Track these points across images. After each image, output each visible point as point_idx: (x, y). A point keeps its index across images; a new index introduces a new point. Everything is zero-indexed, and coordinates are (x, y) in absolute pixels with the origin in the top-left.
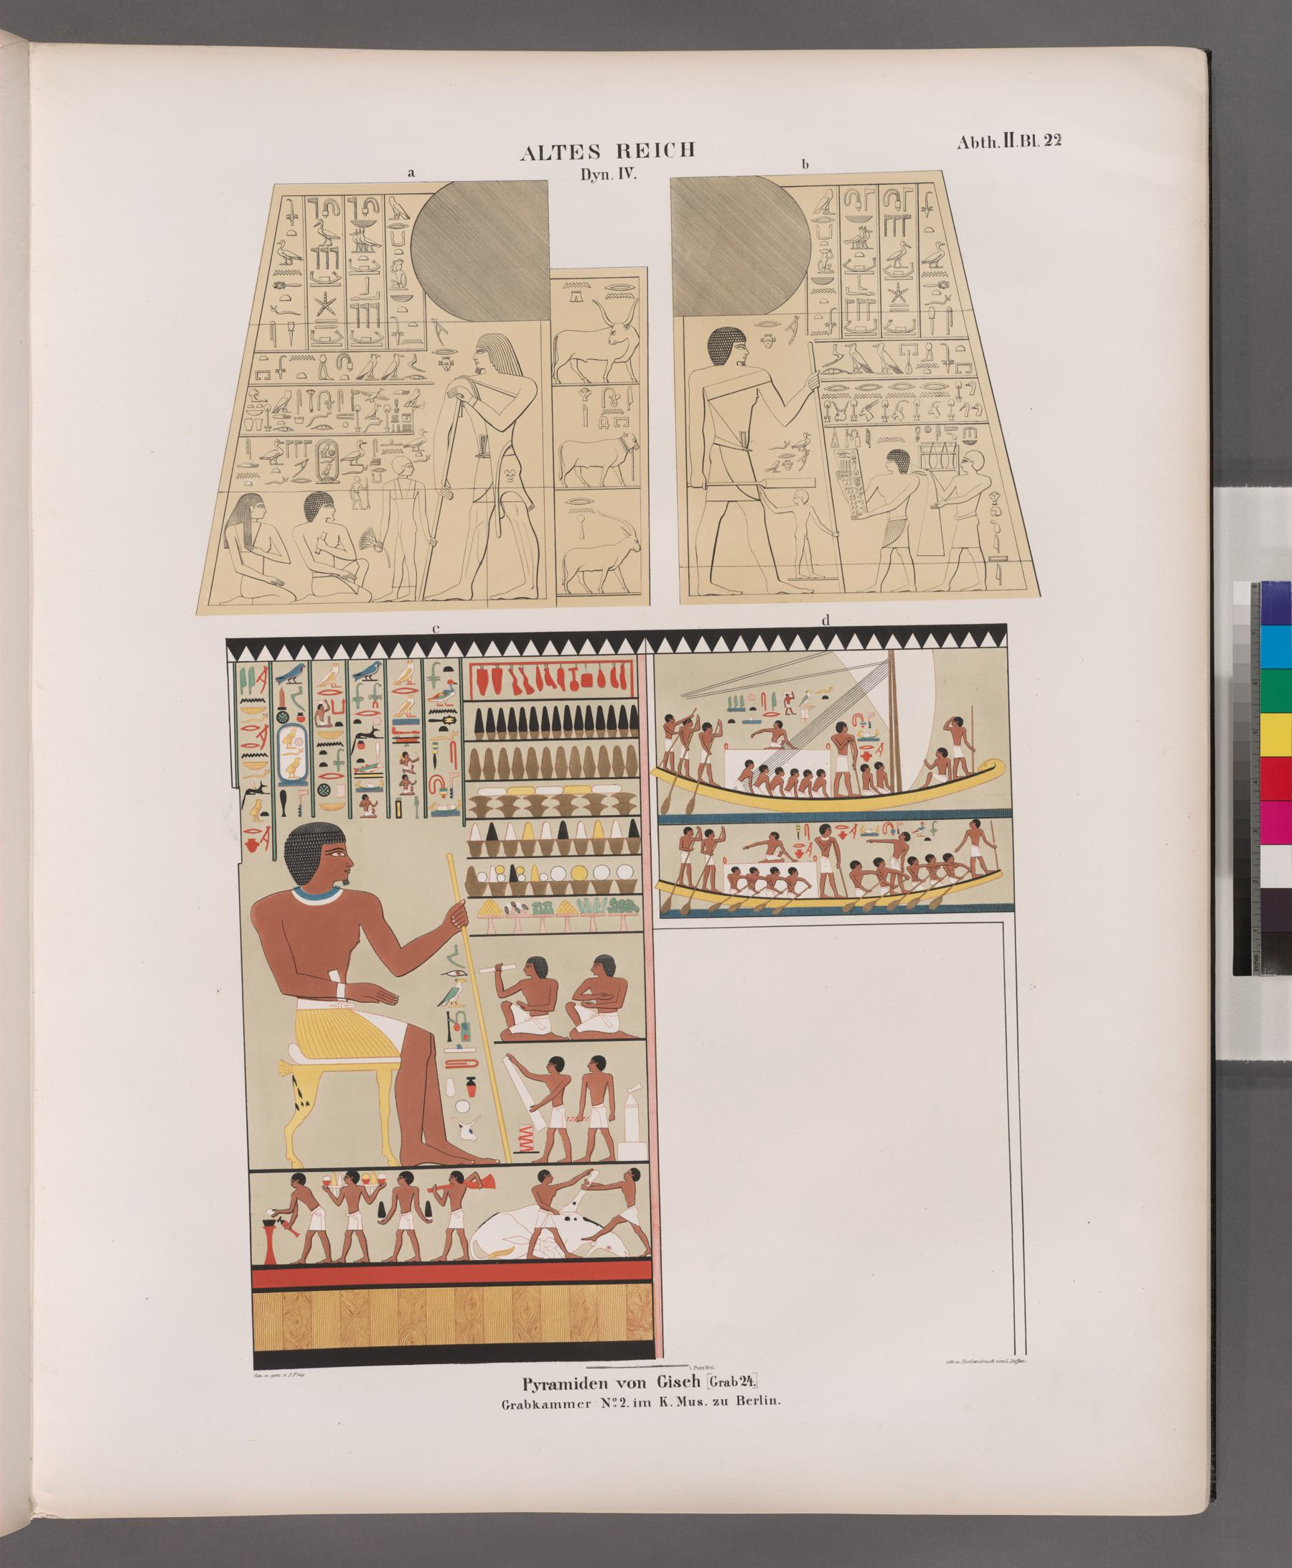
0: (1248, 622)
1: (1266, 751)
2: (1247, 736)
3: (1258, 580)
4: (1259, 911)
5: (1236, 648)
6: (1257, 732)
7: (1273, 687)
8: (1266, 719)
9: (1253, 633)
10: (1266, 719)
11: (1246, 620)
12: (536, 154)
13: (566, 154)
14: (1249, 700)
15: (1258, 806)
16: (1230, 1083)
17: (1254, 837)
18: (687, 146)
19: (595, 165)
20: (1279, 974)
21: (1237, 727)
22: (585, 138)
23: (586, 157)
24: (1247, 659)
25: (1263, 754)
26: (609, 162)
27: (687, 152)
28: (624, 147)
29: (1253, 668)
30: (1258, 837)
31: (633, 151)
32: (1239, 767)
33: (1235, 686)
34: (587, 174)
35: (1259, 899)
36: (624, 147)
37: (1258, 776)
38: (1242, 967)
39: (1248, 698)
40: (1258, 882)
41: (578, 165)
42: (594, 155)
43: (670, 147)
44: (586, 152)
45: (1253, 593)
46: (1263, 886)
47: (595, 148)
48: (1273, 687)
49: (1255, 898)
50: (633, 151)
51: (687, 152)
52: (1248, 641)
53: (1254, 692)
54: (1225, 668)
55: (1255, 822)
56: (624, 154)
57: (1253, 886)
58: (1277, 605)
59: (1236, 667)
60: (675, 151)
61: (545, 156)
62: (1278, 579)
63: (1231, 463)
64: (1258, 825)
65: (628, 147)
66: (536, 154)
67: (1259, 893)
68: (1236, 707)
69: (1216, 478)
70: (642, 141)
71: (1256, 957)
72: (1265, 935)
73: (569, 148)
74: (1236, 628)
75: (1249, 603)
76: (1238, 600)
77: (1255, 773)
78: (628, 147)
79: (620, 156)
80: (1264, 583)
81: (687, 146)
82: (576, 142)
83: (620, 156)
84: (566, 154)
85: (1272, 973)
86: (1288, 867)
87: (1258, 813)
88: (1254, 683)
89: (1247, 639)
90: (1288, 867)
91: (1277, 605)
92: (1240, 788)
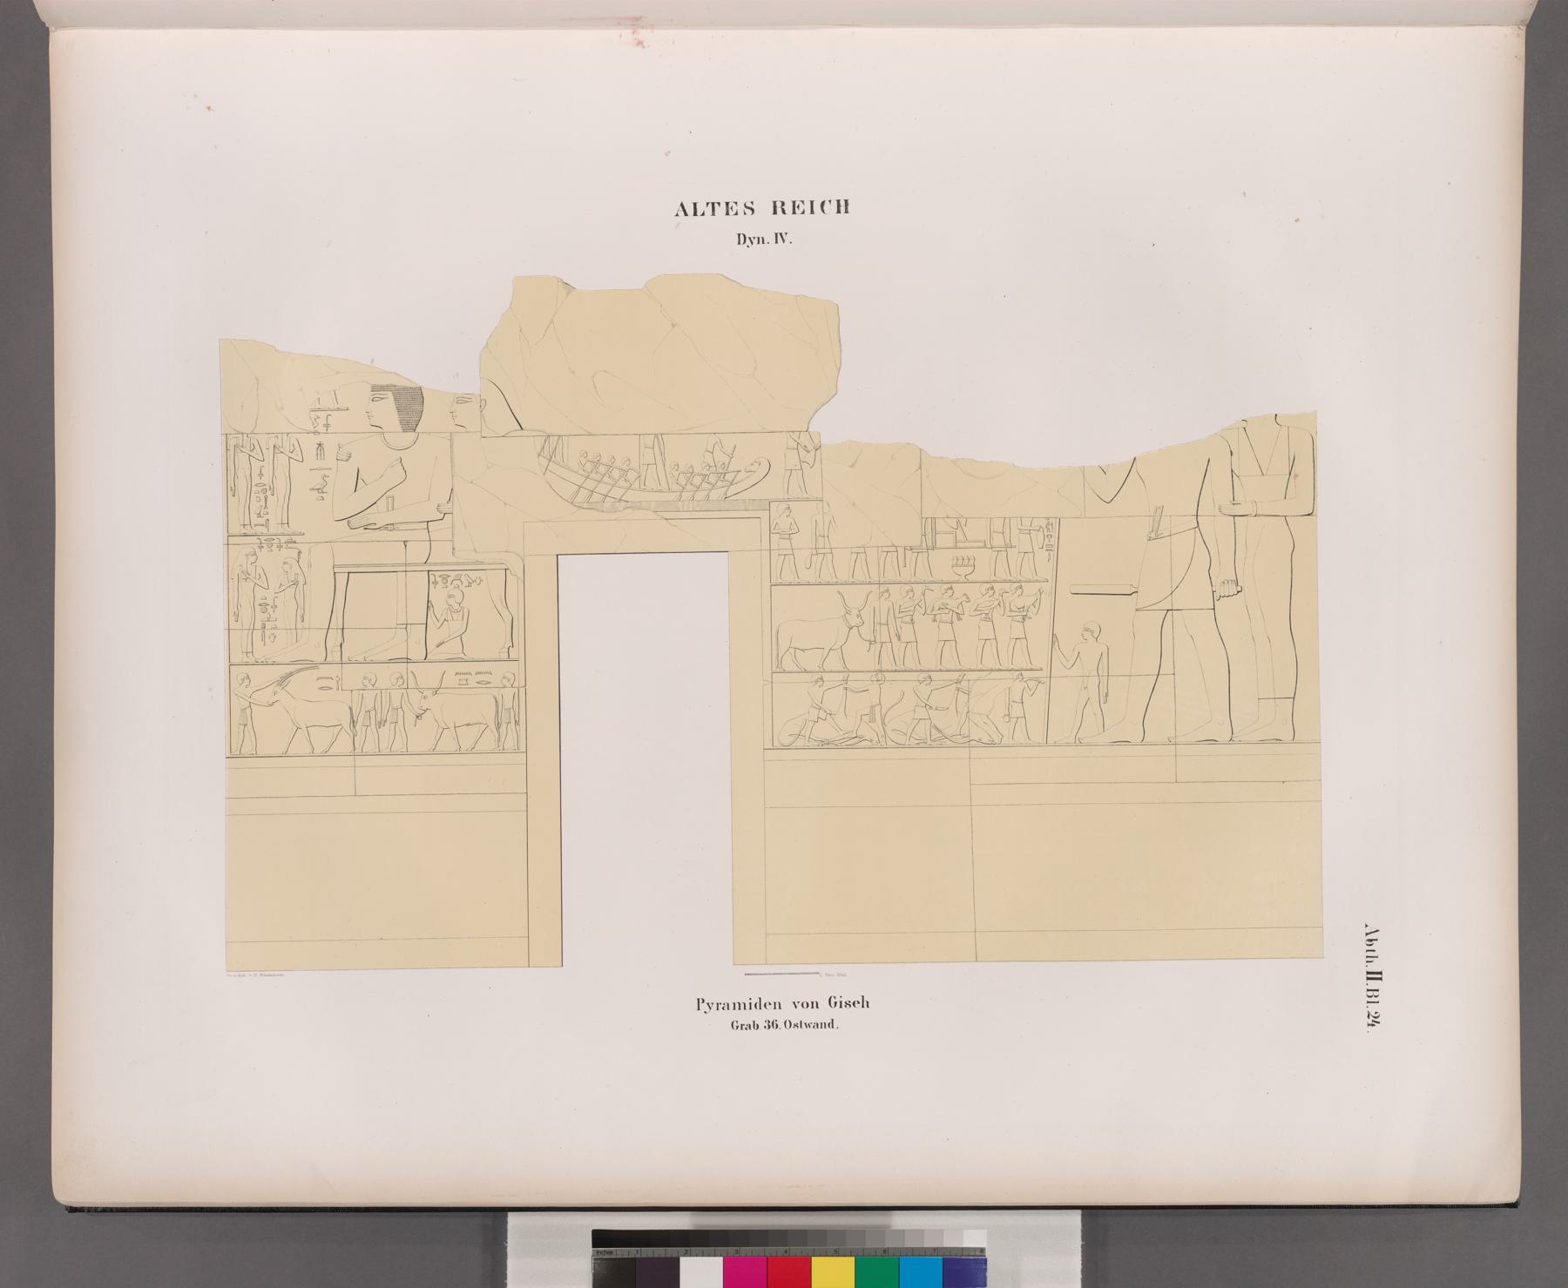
0: (946, 1245)
1: (816, 1262)
2: (832, 1243)
5: (920, 1233)
6: (836, 1253)
8: (850, 1262)
9: (935, 1251)
10: (850, 1262)
11: (949, 1242)
14: (868, 1246)
16: (488, 1222)
17: (731, 1251)
20: (594, 1275)
21: (841, 1234)
29: (900, 1249)
32: (801, 1236)
33: (882, 1231)
39: (870, 1244)
45: (975, 1249)
48: (883, 1271)
49: (670, 1252)
53: (876, 1250)
54: (899, 1221)
55: (746, 1251)
57: (682, 1249)
59: (901, 1233)
62: (989, 1274)
63: (1103, 1223)
68: (861, 1233)
69: (1087, 1210)
72: (633, 1261)
74: (940, 1233)
76: (968, 1234)
77: (796, 1251)
92: (782, 1236)
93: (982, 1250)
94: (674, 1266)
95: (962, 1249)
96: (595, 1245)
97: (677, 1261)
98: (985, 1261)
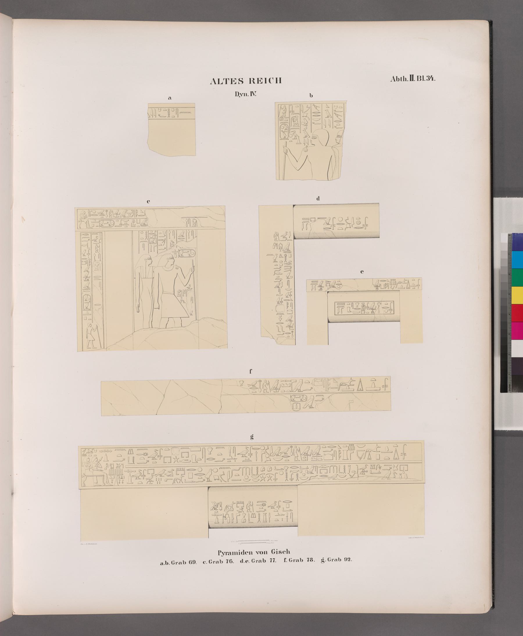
0: (507, 250)
1: (513, 302)
2: (506, 296)
4: (511, 367)
5: (502, 260)
6: (510, 294)
7: (517, 276)
8: (513, 288)
9: (509, 254)
10: (513, 288)
12: (217, 82)
13: (229, 82)
15: (510, 324)
17: (509, 337)
18: (278, 79)
20: (519, 392)
21: (502, 292)
22: (236, 76)
23: (237, 83)
24: (506, 265)
27: (278, 81)
28: (252, 80)
30: (510, 337)
31: (256, 81)
32: (503, 308)
33: (501, 276)
35: (511, 362)
36: (252, 80)
37: (510, 312)
38: (504, 389)
39: (506, 280)
40: (510, 355)
42: (241, 82)
43: (271, 80)
44: (237, 81)
46: (512, 357)
47: (241, 79)
48: (517, 276)
49: (509, 361)
50: (256, 81)
51: (278, 81)
52: (507, 257)
53: (509, 278)
55: (509, 330)
56: (252, 82)
57: (508, 356)
60: (273, 81)
61: (220, 83)
62: (519, 233)
64: (510, 332)
65: (254, 79)
67: (511, 359)
68: (502, 284)
71: (510, 385)
73: (230, 80)
74: (502, 252)
76: (502, 241)
77: (509, 311)
78: (254, 79)
79: (250, 83)
81: (278, 79)
83: (250, 83)
84: (229, 82)
85: (516, 392)
86: (522, 349)
87: (510, 327)
88: (509, 274)
89: (506, 257)
90: (522, 349)
92: (503, 316)
93: (509, 235)
96: (507, 392)
97: (513, 358)
98: (514, 234)
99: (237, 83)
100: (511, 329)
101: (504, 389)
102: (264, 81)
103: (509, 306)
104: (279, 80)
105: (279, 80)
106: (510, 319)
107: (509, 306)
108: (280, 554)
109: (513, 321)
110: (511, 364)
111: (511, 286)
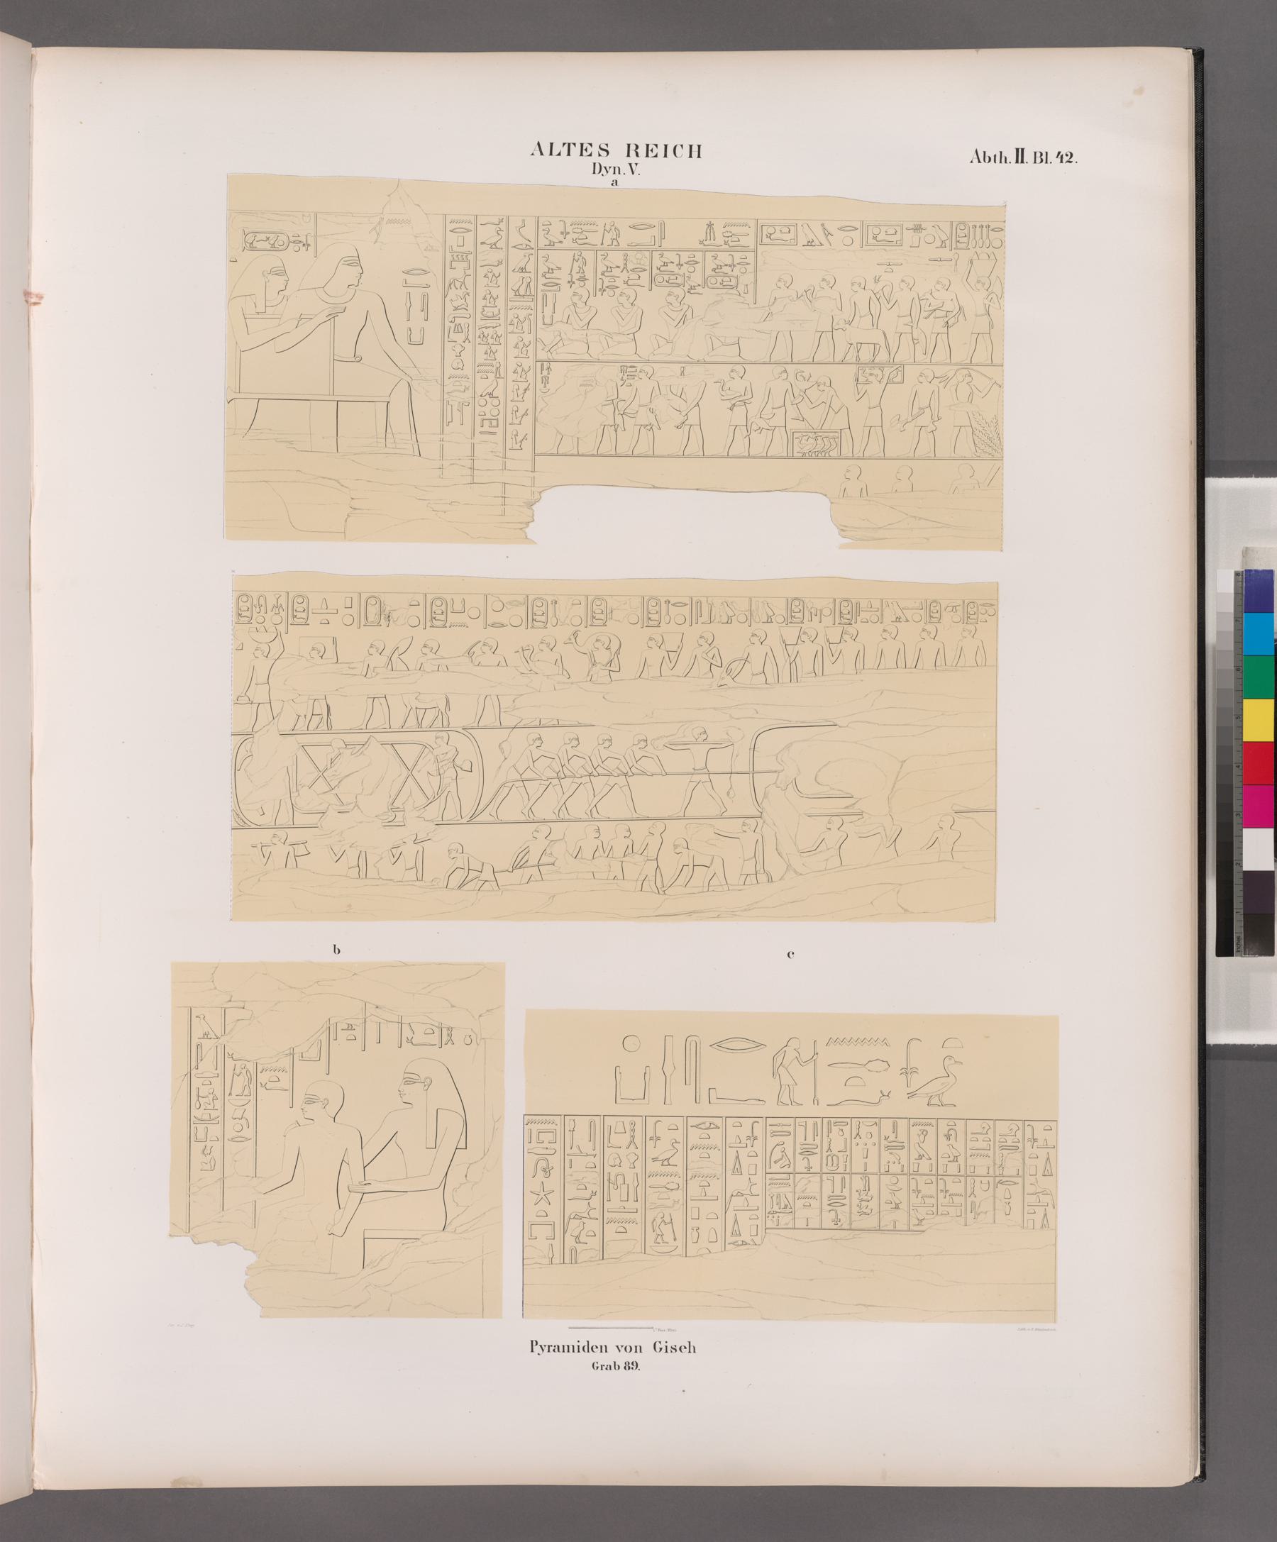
0: (1232, 610)
1: (1249, 736)
3: (1240, 569)
5: (1219, 633)
6: (1240, 717)
8: (1248, 704)
9: (1238, 620)
10: (1248, 704)
11: (1231, 609)
12: (546, 150)
13: (575, 151)
17: (1237, 820)
18: (695, 149)
19: (605, 161)
21: (1220, 711)
23: (595, 155)
24: (1231, 647)
25: (1245, 739)
26: (617, 157)
27: (695, 154)
28: (633, 147)
31: (642, 151)
32: (1222, 751)
34: (598, 169)
35: (1241, 881)
36: (633, 147)
39: (1230, 684)
41: (587, 162)
43: (678, 148)
44: (595, 150)
45: (1236, 582)
46: (1245, 868)
47: (604, 147)
49: (1238, 880)
50: (642, 151)
51: (695, 154)
52: (1232, 629)
53: (1236, 678)
55: (1237, 806)
56: (632, 153)
58: (1256, 591)
61: (555, 152)
62: (1260, 568)
64: (1240, 809)
65: (637, 147)
66: (546, 150)
67: (1241, 875)
69: (1203, 470)
70: (651, 143)
71: (1238, 938)
73: (578, 146)
75: (1232, 591)
76: (1222, 586)
77: (1237, 757)
78: (637, 147)
80: (1248, 571)
81: (695, 149)
82: (586, 141)
84: (575, 151)
87: (1240, 797)
89: (1230, 626)
91: (1256, 591)
94: (1249, 875)
95: (1236, 593)
96: (1232, 955)
99: (595, 155)
100: (1241, 803)
101: (1225, 949)
102: (661, 151)
103: (1236, 748)
104: (695, 151)
105: (695, 151)
106: (1240, 779)
107: (1236, 748)
108: (674, 1353)
109: (1247, 784)
110: (1241, 887)
111: (1243, 698)
